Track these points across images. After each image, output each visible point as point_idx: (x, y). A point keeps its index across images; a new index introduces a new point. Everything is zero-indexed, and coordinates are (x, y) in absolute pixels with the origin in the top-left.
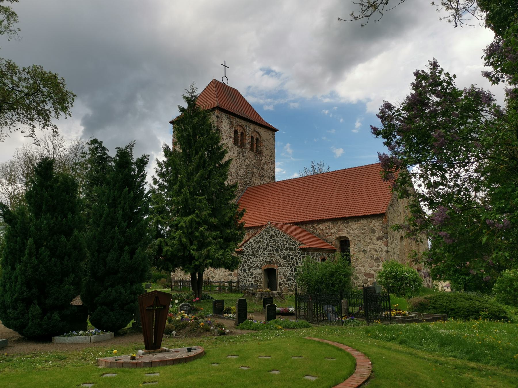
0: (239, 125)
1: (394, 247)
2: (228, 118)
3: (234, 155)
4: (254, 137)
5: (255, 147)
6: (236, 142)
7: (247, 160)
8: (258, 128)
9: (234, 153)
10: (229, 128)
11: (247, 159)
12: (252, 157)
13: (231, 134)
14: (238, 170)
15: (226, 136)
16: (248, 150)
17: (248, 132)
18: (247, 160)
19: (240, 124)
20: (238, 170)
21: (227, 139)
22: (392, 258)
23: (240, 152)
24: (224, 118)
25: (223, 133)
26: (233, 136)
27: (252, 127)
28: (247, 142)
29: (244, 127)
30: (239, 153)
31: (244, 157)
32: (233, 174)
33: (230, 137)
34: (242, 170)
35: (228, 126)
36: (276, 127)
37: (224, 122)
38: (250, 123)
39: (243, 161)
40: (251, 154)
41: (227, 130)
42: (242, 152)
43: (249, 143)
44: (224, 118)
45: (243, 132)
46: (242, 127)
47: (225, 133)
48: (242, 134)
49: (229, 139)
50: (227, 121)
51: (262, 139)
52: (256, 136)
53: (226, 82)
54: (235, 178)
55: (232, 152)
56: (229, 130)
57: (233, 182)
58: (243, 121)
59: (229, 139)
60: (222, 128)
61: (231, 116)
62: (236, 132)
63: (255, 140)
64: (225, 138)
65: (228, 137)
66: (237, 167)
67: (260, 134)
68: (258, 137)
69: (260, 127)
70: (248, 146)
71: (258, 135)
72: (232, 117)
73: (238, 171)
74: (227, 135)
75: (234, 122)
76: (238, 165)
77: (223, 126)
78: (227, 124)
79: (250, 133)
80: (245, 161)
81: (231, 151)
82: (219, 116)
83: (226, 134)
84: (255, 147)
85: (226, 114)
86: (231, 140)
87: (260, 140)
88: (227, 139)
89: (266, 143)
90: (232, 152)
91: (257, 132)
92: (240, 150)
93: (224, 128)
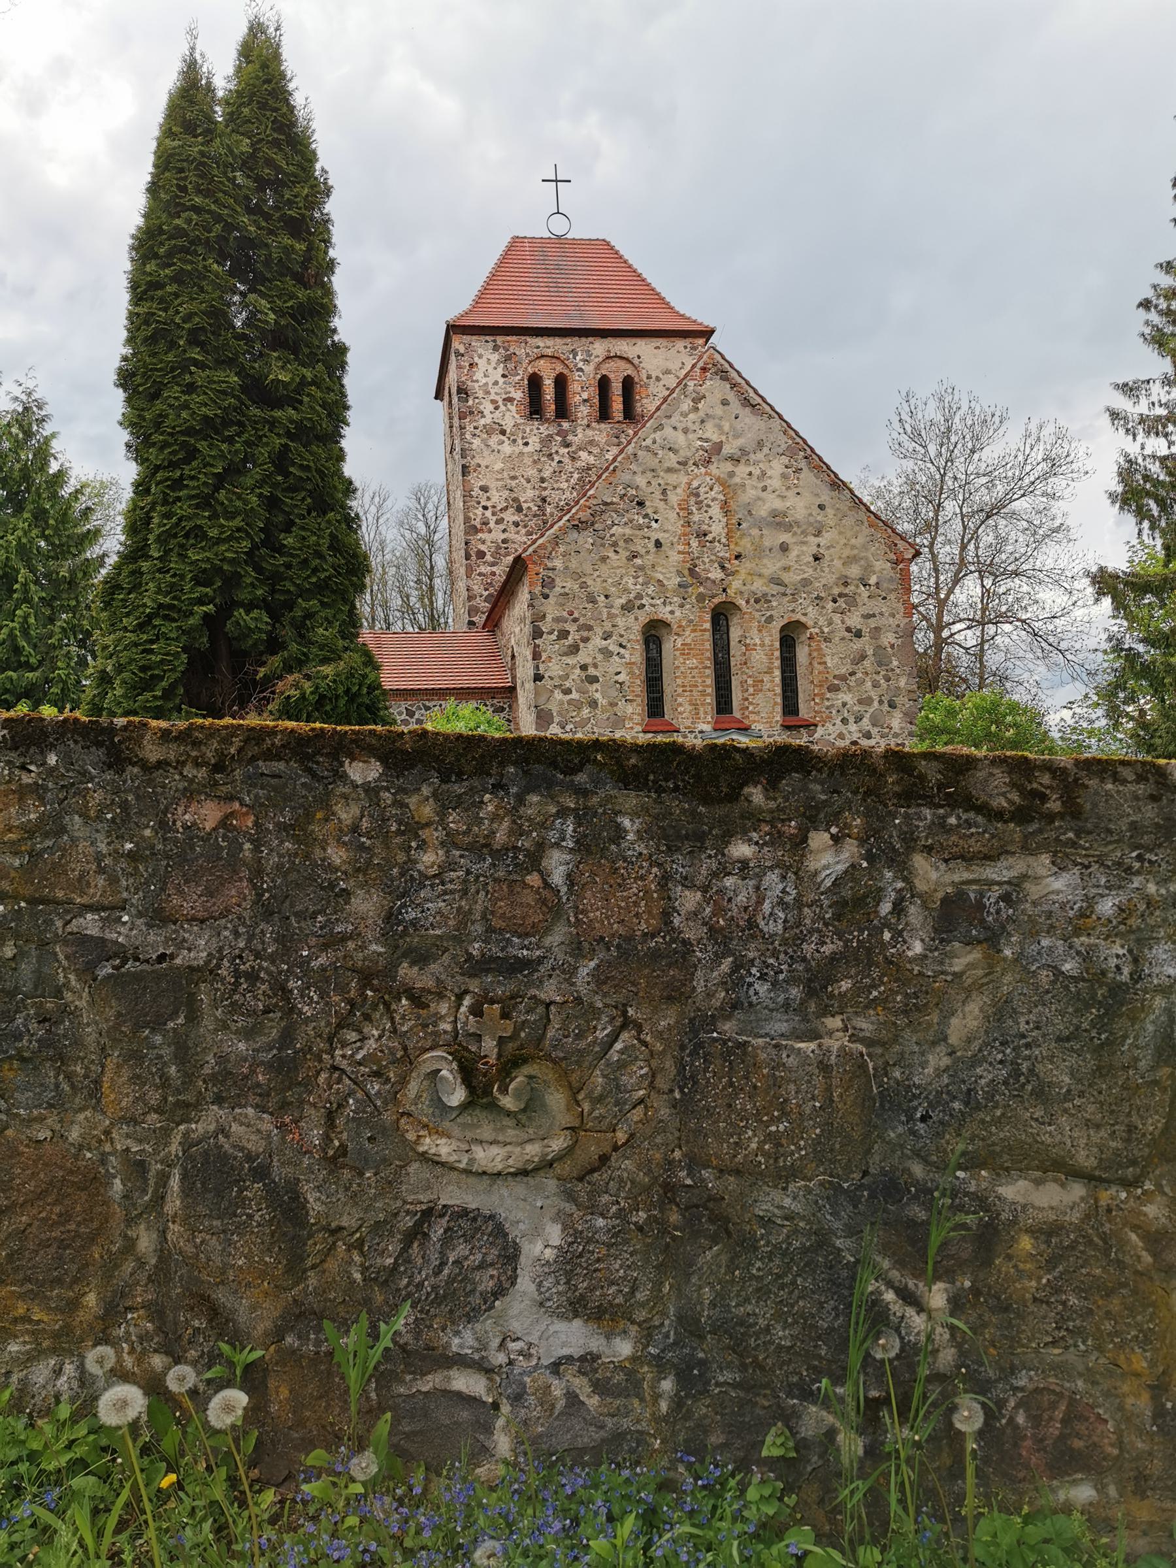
0: (543, 356)
1: (589, 660)
2: (496, 348)
3: (530, 449)
4: (612, 376)
5: (617, 405)
6: (535, 409)
7: (583, 455)
8: (622, 346)
9: (526, 444)
10: (504, 376)
11: (580, 449)
12: (601, 438)
13: (512, 390)
14: (545, 489)
15: (493, 402)
16: (585, 422)
17: (581, 370)
18: (583, 455)
19: (549, 352)
20: (545, 489)
21: (496, 408)
22: (575, 695)
23: (547, 436)
24: (480, 351)
25: (480, 394)
26: (518, 395)
27: (599, 347)
28: (577, 399)
29: (563, 357)
30: (547, 441)
31: (568, 446)
32: (525, 506)
33: (510, 400)
34: (564, 485)
35: (500, 371)
36: (706, 319)
37: (482, 363)
38: (591, 339)
39: (566, 460)
40: (601, 433)
41: (496, 383)
42: (562, 433)
43: (585, 401)
44: (480, 351)
45: (565, 372)
46: (558, 358)
47: (488, 393)
48: (561, 383)
49: (502, 408)
50: (495, 357)
51: (644, 376)
52: (616, 373)
53: (559, 227)
54: (535, 516)
55: (520, 442)
56: (501, 380)
57: (525, 526)
58: (558, 340)
59: (502, 408)
60: (477, 381)
61: (508, 338)
62: (535, 383)
63: (617, 388)
64: (487, 407)
65: (500, 403)
66: (543, 480)
67: (636, 361)
68: (630, 371)
69: (634, 340)
70: (584, 410)
71: (628, 366)
72: (515, 338)
73: (545, 493)
74: (497, 398)
75: (521, 352)
76: (546, 474)
77: (479, 375)
78: (493, 364)
79: (589, 369)
80: (573, 459)
81: (514, 441)
82: (462, 350)
83: (493, 397)
84: (617, 405)
85: (487, 338)
86: (513, 408)
87: (636, 380)
88: (496, 408)
89: (662, 383)
90: (520, 442)
91: (621, 358)
92: (553, 430)
93: (484, 381)
